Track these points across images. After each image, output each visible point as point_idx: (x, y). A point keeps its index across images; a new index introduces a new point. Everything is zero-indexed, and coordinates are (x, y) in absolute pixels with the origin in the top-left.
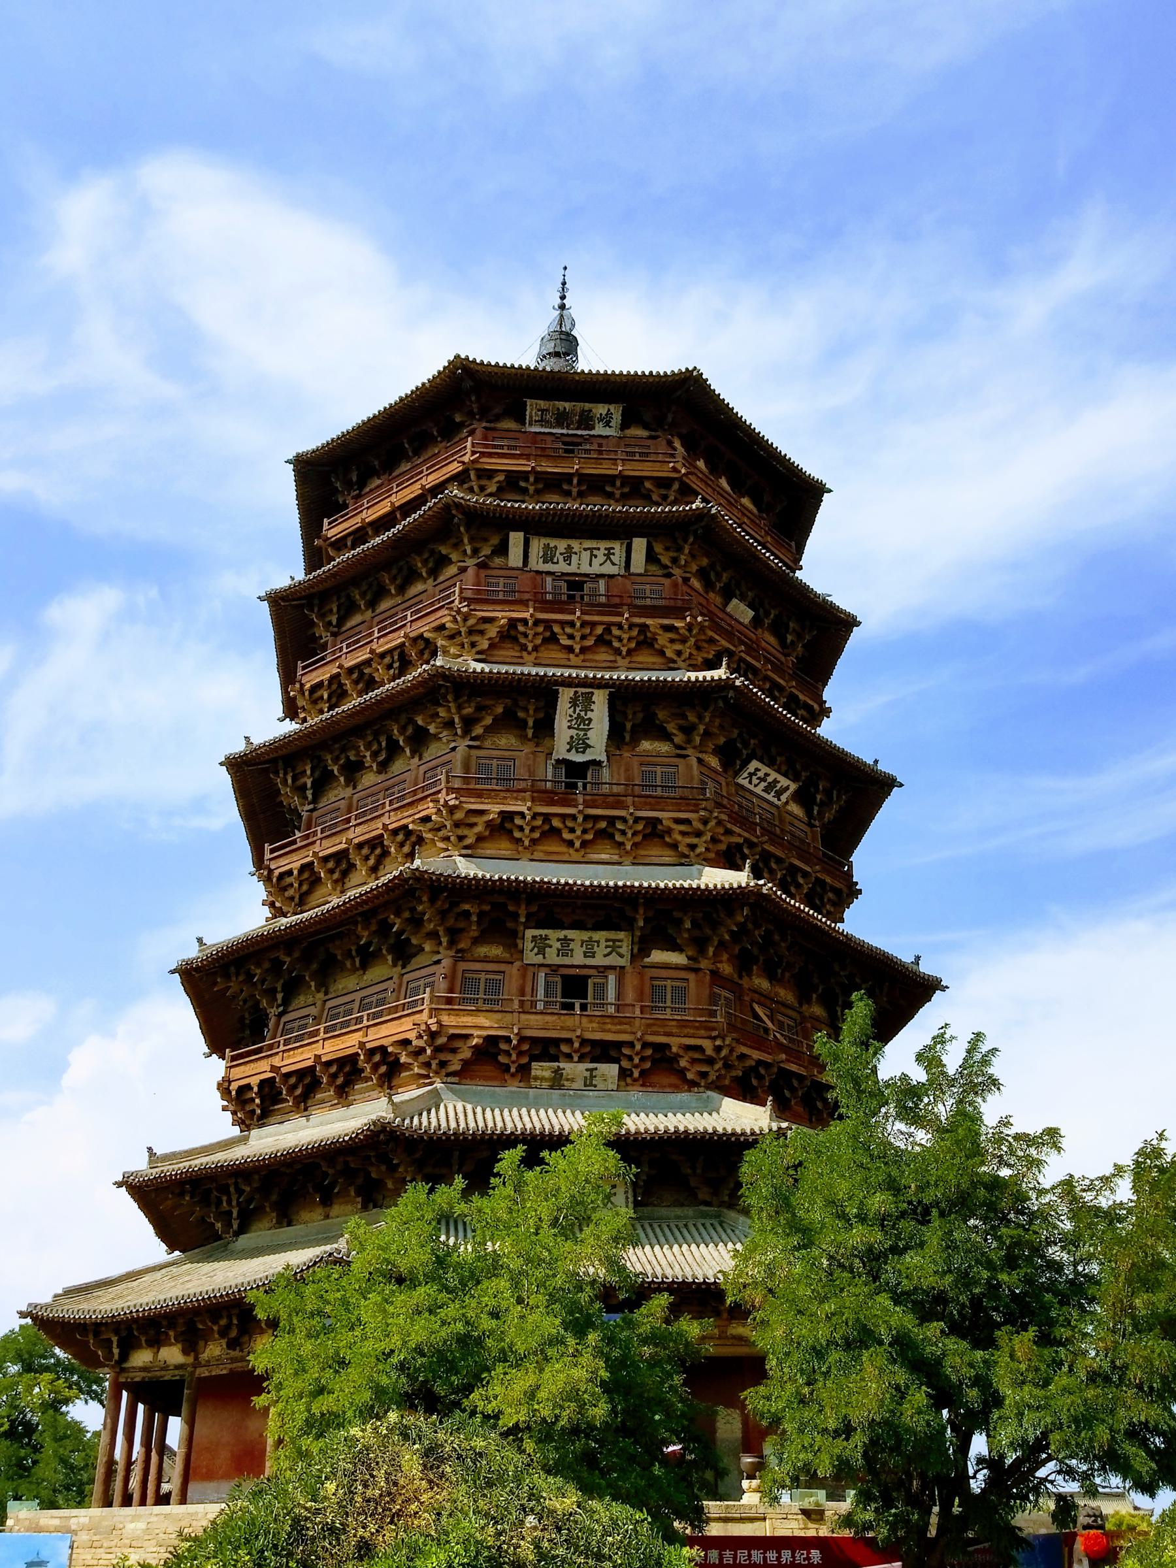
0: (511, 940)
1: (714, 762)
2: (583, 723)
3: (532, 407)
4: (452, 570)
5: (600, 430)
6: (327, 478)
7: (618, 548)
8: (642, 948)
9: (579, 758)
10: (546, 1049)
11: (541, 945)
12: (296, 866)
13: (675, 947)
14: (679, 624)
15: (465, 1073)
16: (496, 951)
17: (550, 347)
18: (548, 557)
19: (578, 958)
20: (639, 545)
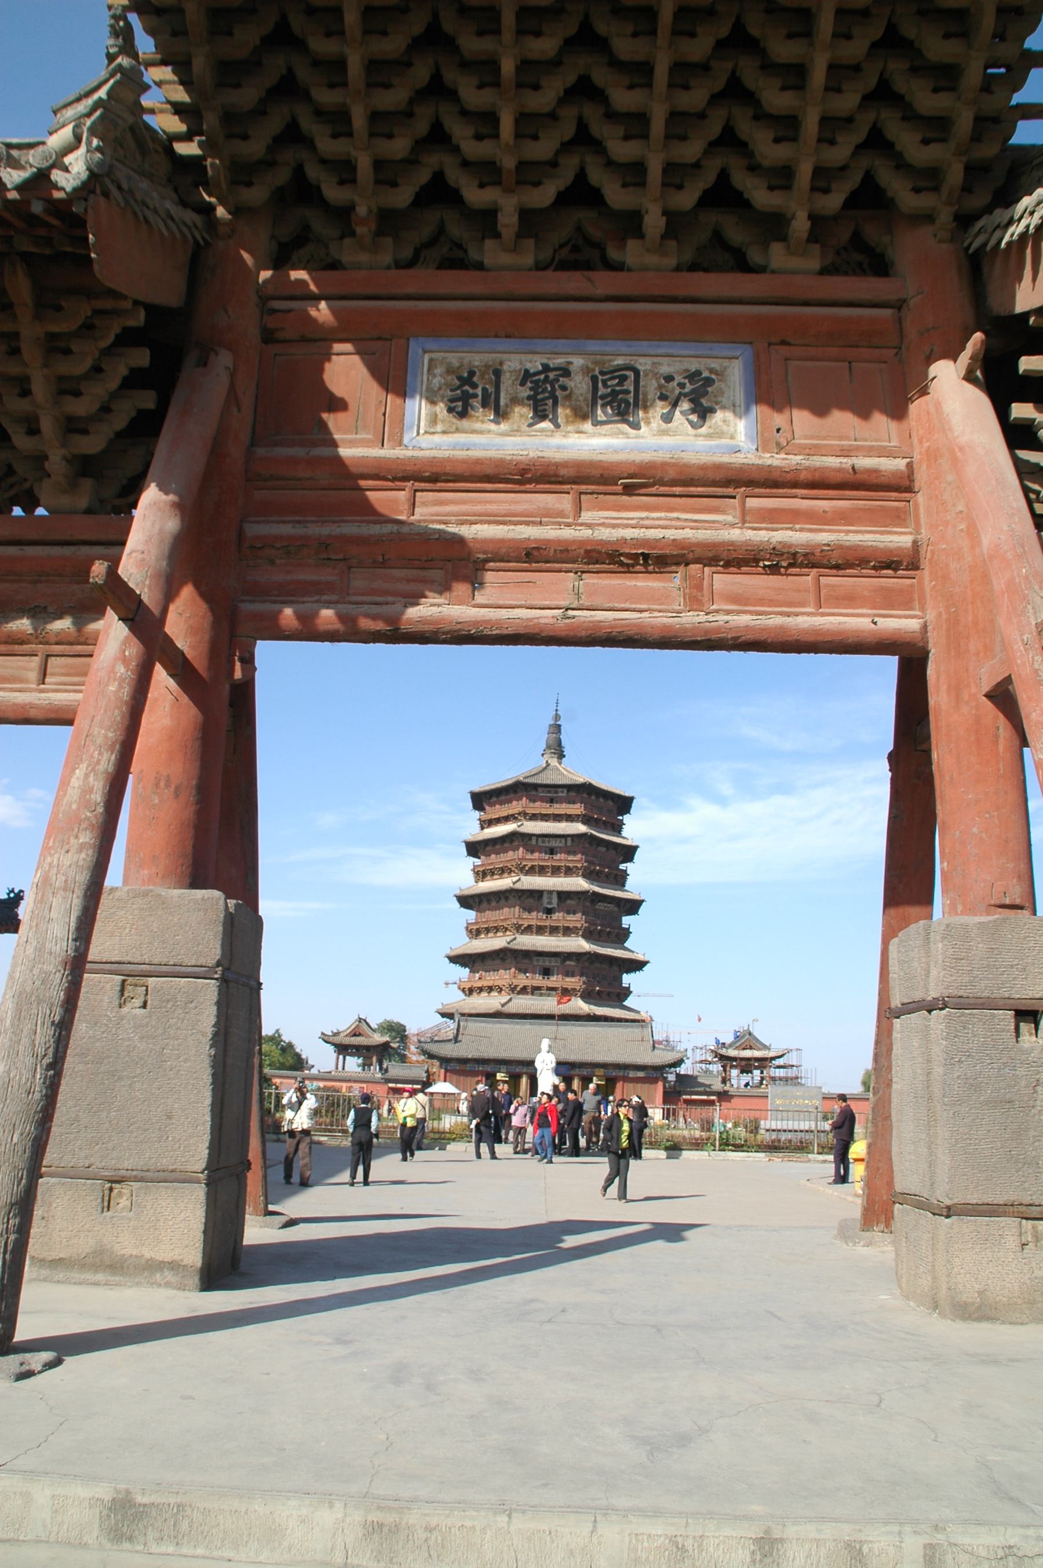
0: (531, 959)
1: (588, 904)
2: (550, 898)
3: (540, 789)
4: (516, 843)
5: (560, 794)
6: (480, 800)
7: (563, 840)
8: (564, 960)
9: (549, 906)
10: (539, 988)
11: (538, 961)
12: (475, 927)
13: (571, 960)
14: (579, 865)
15: (519, 993)
16: (526, 961)
17: (552, 730)
18: (543, 842)
19: (547, 964)
20: (569, 839)
